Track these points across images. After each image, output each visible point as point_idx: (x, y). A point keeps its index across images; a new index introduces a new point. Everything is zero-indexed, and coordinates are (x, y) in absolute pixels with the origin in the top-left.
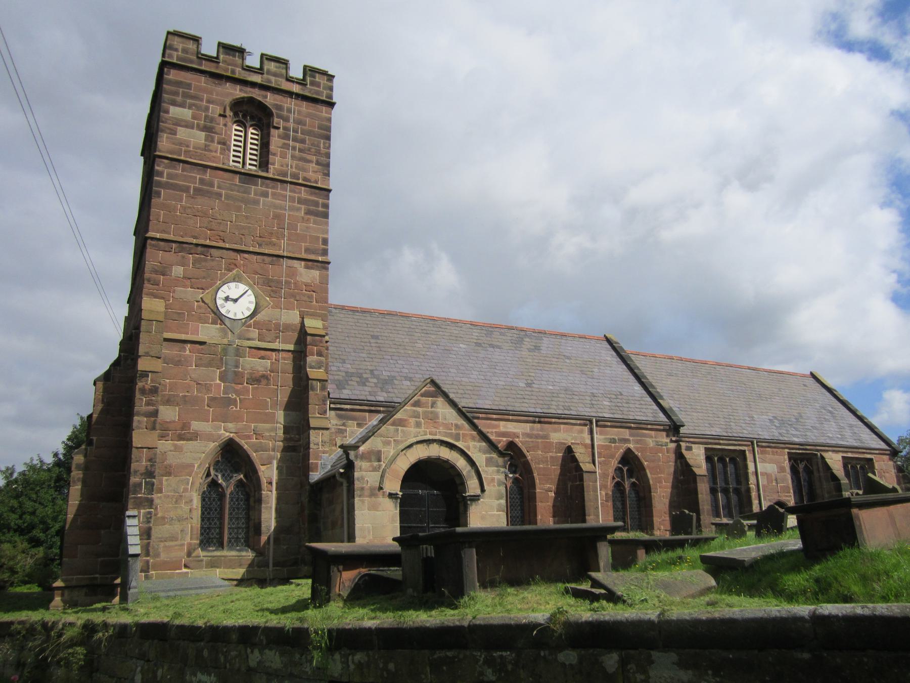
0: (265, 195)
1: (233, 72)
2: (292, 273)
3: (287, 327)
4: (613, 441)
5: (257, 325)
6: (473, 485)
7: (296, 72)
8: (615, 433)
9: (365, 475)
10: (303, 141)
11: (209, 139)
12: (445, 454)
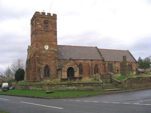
0: (49, 33)
1: (44, 16)
2: (53, 43)
3: (53, 50)
4: (95, 62)
5: (49, 50)
6: (75, 70)
7: (52, 15)
8: (95, 61)
9: (63, 69)
10: (53, 25)
11: (42, 26)
12: (72, 66)
